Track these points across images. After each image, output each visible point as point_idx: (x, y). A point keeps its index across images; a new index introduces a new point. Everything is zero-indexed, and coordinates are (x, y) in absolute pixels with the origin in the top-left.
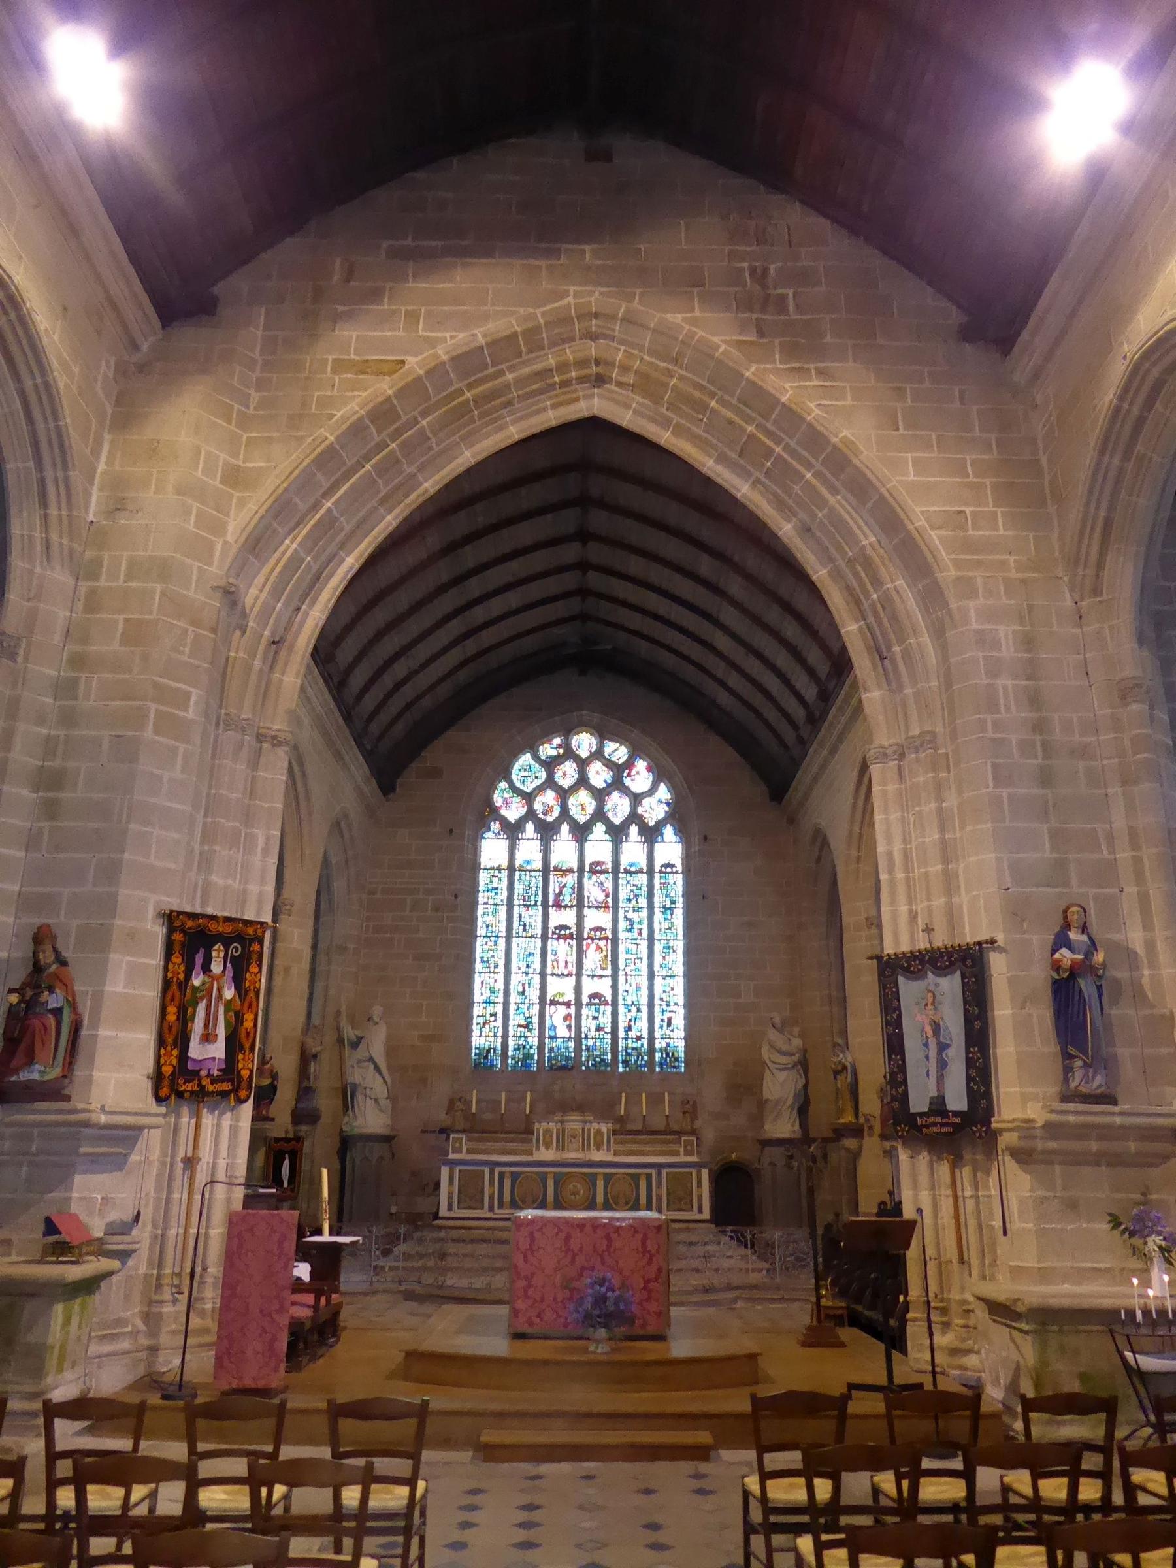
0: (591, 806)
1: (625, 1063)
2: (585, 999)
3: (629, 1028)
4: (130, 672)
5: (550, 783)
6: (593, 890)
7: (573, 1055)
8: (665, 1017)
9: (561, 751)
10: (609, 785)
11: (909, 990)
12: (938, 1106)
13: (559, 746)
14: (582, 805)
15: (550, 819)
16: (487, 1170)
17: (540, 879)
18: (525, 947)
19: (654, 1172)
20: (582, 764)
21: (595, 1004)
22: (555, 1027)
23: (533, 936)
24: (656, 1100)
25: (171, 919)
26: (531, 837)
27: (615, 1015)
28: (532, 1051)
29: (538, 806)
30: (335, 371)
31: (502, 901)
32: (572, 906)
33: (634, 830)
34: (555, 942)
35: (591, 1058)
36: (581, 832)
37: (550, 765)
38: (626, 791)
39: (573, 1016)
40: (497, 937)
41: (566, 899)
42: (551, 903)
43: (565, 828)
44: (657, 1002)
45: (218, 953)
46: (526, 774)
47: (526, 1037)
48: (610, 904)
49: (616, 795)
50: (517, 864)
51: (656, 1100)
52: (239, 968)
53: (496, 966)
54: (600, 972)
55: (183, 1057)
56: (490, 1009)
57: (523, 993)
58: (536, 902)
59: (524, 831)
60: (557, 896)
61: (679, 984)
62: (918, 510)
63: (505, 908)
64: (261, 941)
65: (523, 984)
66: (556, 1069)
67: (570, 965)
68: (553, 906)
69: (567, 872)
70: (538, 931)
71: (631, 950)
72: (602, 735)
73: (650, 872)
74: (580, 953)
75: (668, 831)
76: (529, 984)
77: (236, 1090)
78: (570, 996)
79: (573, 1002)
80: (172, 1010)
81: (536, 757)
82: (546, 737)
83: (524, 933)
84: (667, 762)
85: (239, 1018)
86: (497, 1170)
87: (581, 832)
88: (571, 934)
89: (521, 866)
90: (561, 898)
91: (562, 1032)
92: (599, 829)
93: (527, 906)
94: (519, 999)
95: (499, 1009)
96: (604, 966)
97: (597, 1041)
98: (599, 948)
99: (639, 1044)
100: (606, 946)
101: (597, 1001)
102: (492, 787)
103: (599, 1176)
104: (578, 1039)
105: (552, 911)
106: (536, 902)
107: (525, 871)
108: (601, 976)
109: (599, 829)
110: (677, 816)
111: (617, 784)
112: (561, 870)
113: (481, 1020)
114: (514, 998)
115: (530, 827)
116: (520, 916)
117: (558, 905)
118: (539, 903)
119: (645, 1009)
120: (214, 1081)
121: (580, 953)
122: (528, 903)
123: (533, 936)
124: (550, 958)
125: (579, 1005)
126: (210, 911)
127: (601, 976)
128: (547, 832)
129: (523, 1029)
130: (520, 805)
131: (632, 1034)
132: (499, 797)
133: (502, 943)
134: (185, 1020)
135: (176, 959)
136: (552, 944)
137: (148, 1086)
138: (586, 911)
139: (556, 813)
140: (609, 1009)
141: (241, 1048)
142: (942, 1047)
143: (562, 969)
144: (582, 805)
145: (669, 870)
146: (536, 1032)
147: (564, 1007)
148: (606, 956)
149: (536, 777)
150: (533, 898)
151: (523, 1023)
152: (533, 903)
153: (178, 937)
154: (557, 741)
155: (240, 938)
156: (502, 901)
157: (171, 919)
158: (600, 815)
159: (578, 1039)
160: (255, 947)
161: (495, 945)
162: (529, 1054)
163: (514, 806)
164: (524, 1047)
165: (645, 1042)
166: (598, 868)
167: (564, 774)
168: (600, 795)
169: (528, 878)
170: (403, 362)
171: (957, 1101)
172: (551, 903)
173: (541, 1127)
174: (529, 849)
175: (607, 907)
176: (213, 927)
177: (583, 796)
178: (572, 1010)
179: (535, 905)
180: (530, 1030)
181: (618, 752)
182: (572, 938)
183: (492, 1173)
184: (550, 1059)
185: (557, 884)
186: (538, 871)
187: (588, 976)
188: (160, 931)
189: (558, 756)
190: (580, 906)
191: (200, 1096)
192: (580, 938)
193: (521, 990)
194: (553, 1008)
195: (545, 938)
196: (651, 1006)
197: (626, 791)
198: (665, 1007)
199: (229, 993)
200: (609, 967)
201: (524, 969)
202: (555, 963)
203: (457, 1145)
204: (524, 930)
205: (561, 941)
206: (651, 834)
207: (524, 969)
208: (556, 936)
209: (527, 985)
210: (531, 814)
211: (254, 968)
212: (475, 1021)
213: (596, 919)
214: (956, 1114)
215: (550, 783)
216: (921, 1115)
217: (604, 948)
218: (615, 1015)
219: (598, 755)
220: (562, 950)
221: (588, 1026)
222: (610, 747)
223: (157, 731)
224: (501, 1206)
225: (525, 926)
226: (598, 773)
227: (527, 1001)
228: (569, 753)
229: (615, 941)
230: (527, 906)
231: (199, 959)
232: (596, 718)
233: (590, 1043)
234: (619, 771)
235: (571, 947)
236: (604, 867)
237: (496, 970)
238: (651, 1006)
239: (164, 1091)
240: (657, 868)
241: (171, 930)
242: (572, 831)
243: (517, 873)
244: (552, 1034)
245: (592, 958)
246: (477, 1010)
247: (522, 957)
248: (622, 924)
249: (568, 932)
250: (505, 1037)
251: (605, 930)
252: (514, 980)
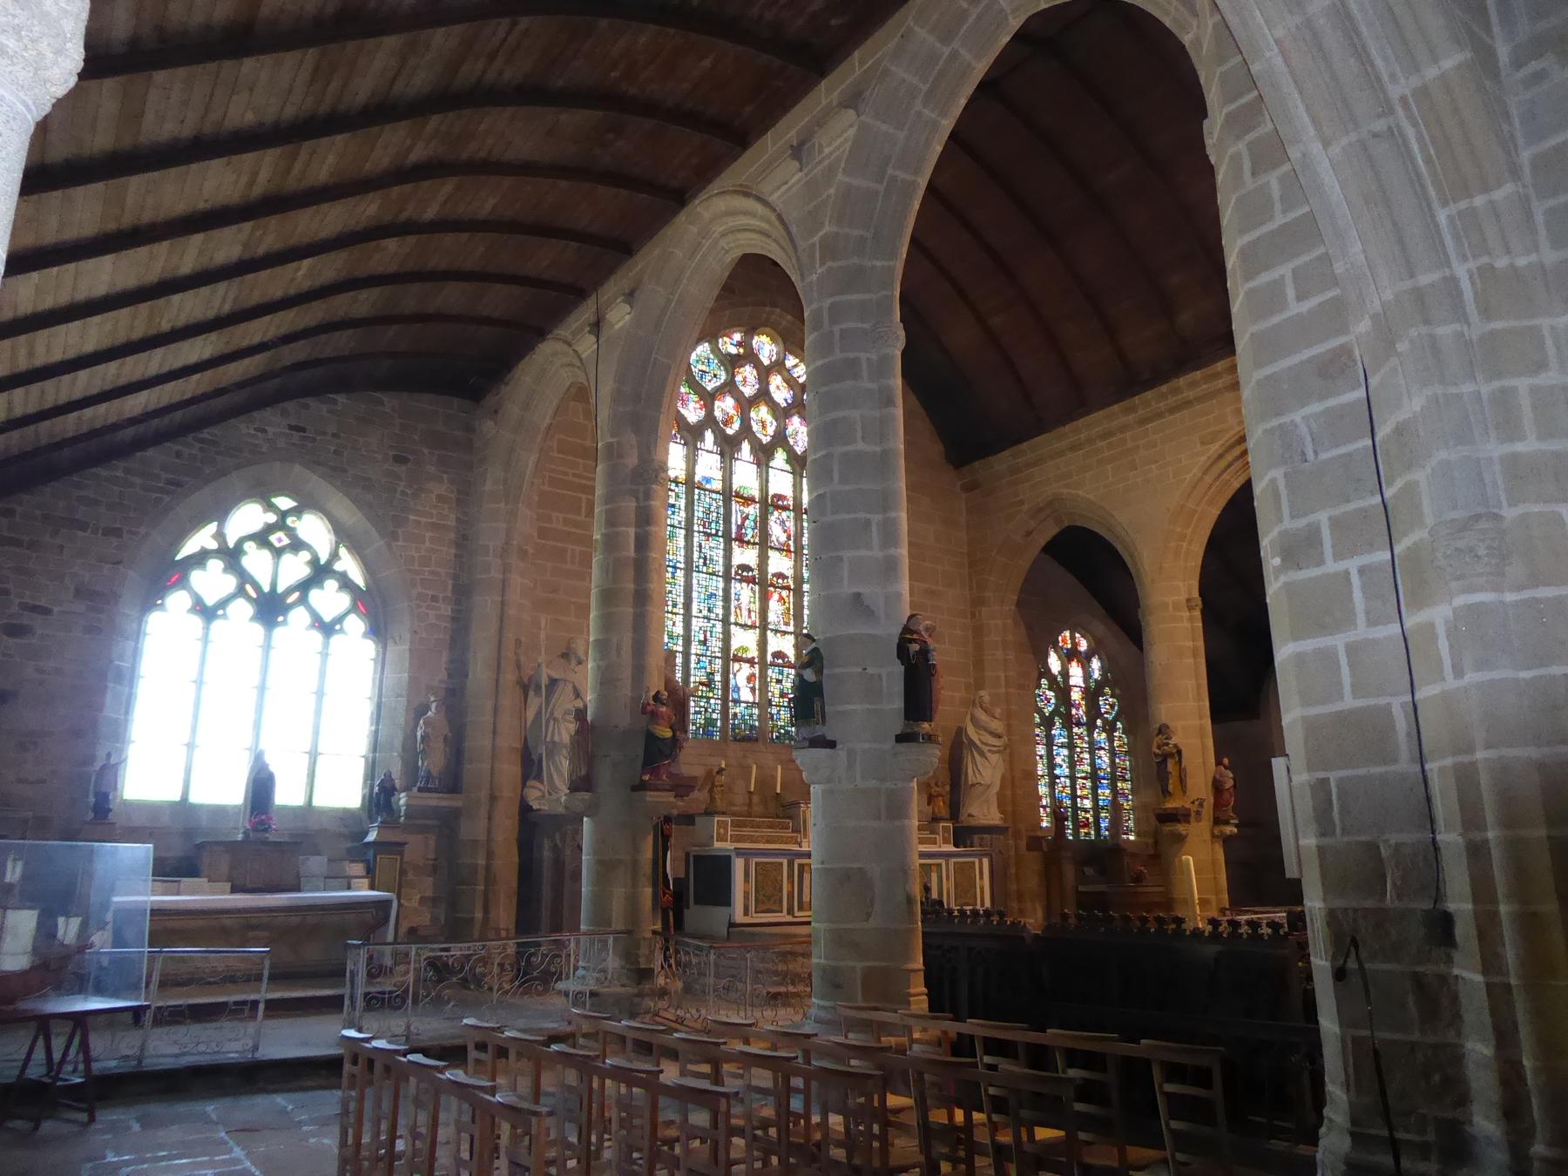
2: (769, 658)
7: (757, 724)
9: (741, 350)
13: (739, 344)
15: (730, 431)
16: (785, 862)
17: (721, 503)
19: (943, 862)
20: (764, 373)
21: (778, 665)
22: (739, 689)
23: (713, 574)
26: (710, 449)
28: (714, 716)
31: (680, 522)
32: (754, 544)
34: (738, 585)
35: (775, 729)
36: (763, 455)
37: (732, 363)
39: (757, 675)
40: (675, 567)
41: (749, 534)
42: (733, 536)
46: (704, 368)
47: (709, 698)
48: (792, 549)
50: (697, 478)
53: (675, 605)
54: (783, 628)
57: (704, 642)
58: (717, 531)
59: (703, 440)
60: (740, 527)
63: (683, 532)
65: (705, 632)
66: (739, 740)
67: (753, 614)
68: (736, 540)
69: (749, 500)
70: (720, 568)
74: (764, 599)
76: (711, 632)
78: (753, 652)
79: (756, 660)
81: (716, 350)
83: (705, 569)
86: (797, 862)
88: (754, 577)
89: (699, 482)
90: (743, 531)
91: (746, 695)
93: (708, 535)
96: (786, 620)
98: (781, 598)
100: (788, 596)
101: (780, 661)
103: (933, 867)
105: (735, 545)
106: (717, 531)
107: (705, 490)
108: (785, 633)
109: (780, 458)
112: (742, 497)
114: (695, 648)
116: (700, 546)
117: (741, 540)
118: (720, 533)
121: (764, 599)
122: (709, 531)
123: (713, 574)
124: (734, 603)
127: (785, 633)
129: (704, 689)
130: (698, 406)
133: (680, 574)
136: (736, 587)
139: (736, 426)
143: (744, 619)
147: (748, 665)
148: (788, 609)
149: (715, 376)
150: (713, 525)
151: (704, 679)
152: (714, 532)
154: (737, 337)
156: (680, 522)
161: (673, 578)
162: (711, 719)
163: (692, 405)
164: (706, 711)
166: (780, 502)
167: (745, 379)
169: (707, 500)
172: (733, 536)
174: (709, 465)
175: (789, 551)
177: (761, 413)
178: (756, 670)
179: (716, 535)
180: (711, 690)
182: (755, 583)
183: (791, 865)
184: (733, 730)
185: (739, 514)
186: (717, 493)
187: (772, 630)
189: (738, 355)
193: (702, 638)
194: (737, 666)
200: (792, 622)
201: (705, 613)
202: (738, 611)
203: (722, 831)
204: (705, 564)
205: (744, 585)
207: (705, 613)
208: (738, 577)
209: (708, 634)
217: (786, 599)
219: (778, 366)
220: (745, 594)
222: (791, 361)
224: (801, 908)
225: (705, 559)
226: (778, 387)
227: (709, 653)
228: (750, 357)
230: (708, 535)
235: (754, 592)
236: (785, 503)
237: (675, 610)
242: (753, 451)
244: (735, 696)
247: (702, 597)
249: (750, 574)
251: (787, 578)
252: (696, 624)
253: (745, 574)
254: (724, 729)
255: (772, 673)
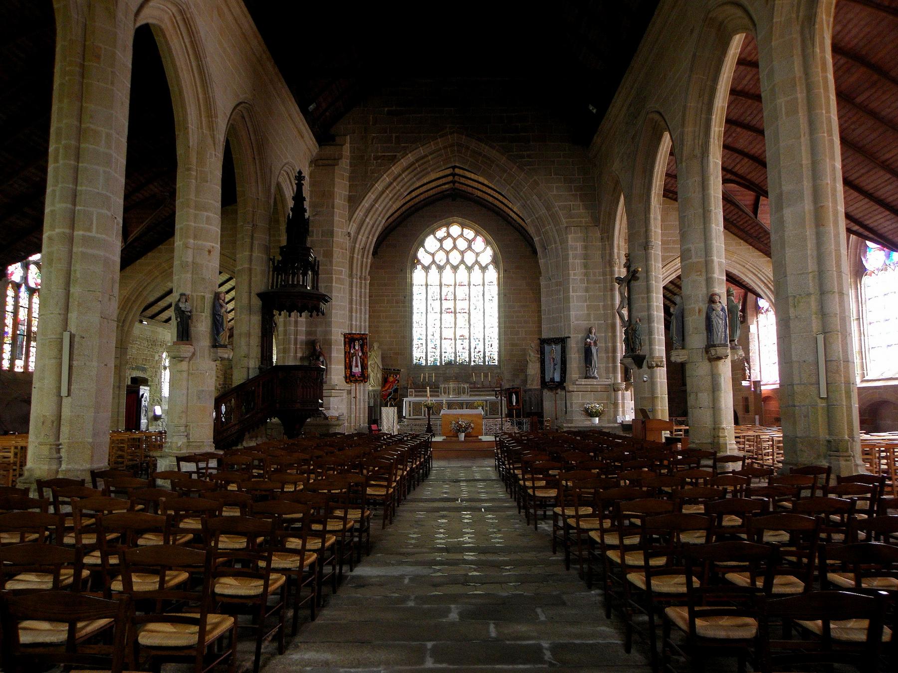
0: (459, 257)
1: (474, 361)
2: (458, 337)
3: (475, 348)
4: (326, 266)
5: (441, 248)
6: (461, 292)
8: (490, 343)
10: (466, 249)
11: (547, 348)
12: (552, 380)
14: (455, 258)
15: (442, 264)
18: (433, 317)
24: (486, 376)
25: (345, 335)
27: (470, 343)
29: (437, 259)
30: (374, 159)
33: (477, 267)
36: (455, 268)
38: (473, 251)
43: (448, 267)
44: (486, 337)
45: (357, 343)
49: (469, 252)
51: (486, 376)
52: (362, 347)
55: (351, 371)
56: (421, 342)
61: (496, 330)
62: (556, 204)
64: (367, 339)
70: (439, 311)
71: (476, 317)
72: (463, 226)
73: (484, 285)
75: (491, 267)
77: (364, 379)
80: (347, 359)
82: (439, 228)
84: (490, 238)
85: (363, 360)
87: (455, 268)
92: (462, 267)
94: (432, 337)
95: (424, 342)
97: (464, 357)
99: (479, 354)
101: (462, 338)
102: (417, 250)
104: (455, 353)
109: (462, 267)
110: (495, 261)
111: (470, 247)
113: (417, 346)
115: (433, 267)
119: (482, 341)
120: (359, 377)
125: (455, 340)
126: (354, 332)
128: (441, 268)
131: (477, 350)
132: (421, 254)
134: (351, 362)
135: (347, 346)
137: (344, 379)
138: (457, 301)
139: (445, 261)
140: (468, 341)
141: (365, 369)
142: (555, 365)
144: (455, 258)
145: (491, 284)
146: (439, 350)
153: (347, 340)
154: (444, 229)
155: (362, 339)
157: (345, 335)
158: (462, 262)
159: (455, 353)
160: (365, 341)
165: (482, 353)
168: (462, 253)
170: (396, 156)
171: (557, 378)
173: (442, 386)
176: (355, 336)
181: (469, 233)
188: (343, 339)
189: (445, 237)
190: (455, 299)
191: (356, 381)
192: (455, 313)
195: (441, 313)
196: (484, 339)
197: (473, 251)
198: (490, 340)
199: (360, 354)
206: (484, 269)
210: (434, 262)
211: (365, 347)
212: (414, 346)
213: (461, 305)
214: (557, 382)
215: (441, 248)
216: (548, 382)
218: (470, 343)
219: (462, 235)
220: (448, 318)
221: (459, 348)
222: (466, 231)
223: (336, 283)
228: (449, 235)
229: (469, 314)
231: (352, 345)
232: (460, 220)
233: (460, 354)
234: (470, 242)
238: (484, 339)
239: (348, 381)
240: (486, 283)
241: (345, 338)
243: (429, 286)
245: (462, 319)
246: (415, 342)
248: (472, 308)
249: (450, 310)
250: (426, 353)
253: (448, 310)
254: (441, 362)
255: (459, 342)
